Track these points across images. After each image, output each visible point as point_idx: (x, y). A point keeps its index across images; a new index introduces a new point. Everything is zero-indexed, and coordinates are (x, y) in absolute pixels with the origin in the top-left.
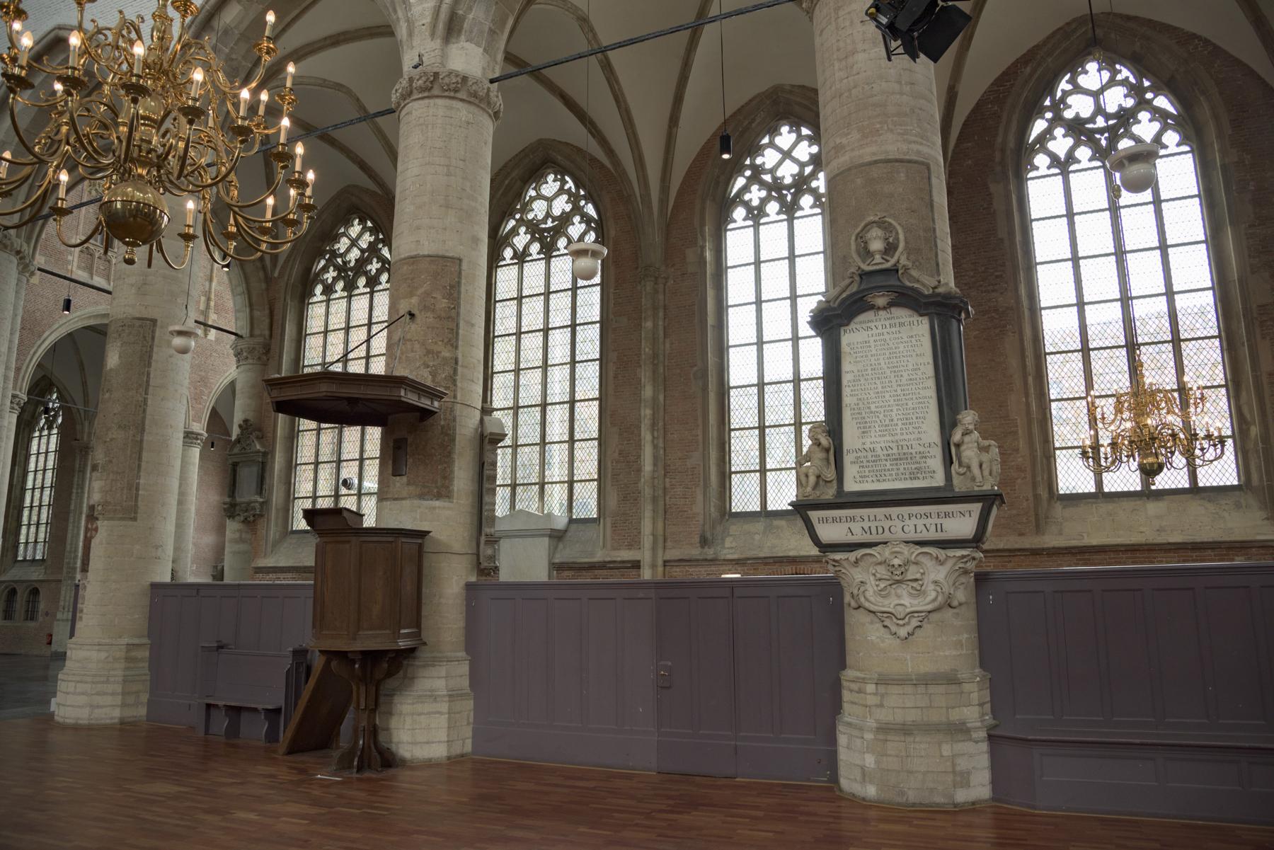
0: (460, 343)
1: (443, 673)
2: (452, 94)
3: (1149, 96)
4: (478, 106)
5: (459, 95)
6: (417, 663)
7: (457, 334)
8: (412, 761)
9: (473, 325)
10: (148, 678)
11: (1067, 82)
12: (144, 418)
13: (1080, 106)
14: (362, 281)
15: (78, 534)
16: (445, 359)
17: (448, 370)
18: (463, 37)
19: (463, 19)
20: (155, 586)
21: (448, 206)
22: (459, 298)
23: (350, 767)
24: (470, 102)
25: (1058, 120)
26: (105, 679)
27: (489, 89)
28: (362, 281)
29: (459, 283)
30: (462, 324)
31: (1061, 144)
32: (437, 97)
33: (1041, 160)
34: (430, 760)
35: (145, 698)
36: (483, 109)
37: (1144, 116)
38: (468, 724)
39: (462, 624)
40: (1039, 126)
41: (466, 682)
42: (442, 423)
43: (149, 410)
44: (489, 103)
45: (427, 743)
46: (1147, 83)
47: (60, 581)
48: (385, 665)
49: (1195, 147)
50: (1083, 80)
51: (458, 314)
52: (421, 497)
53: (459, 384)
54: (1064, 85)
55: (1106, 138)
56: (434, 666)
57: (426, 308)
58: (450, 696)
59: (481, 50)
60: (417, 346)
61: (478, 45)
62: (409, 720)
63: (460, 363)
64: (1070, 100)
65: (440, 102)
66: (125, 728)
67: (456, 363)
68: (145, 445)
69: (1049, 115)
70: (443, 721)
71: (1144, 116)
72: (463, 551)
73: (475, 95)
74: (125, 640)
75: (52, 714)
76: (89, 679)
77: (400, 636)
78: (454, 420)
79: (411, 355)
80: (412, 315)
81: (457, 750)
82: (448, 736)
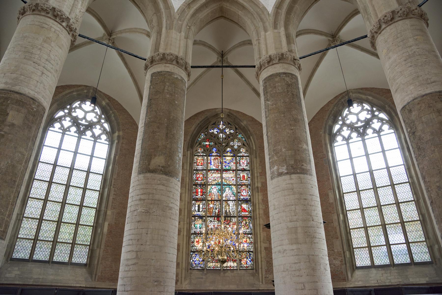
3: (103, 121)
11: (78, 104)
13: (79, 113)
25: (70, 114)
31: (67, 123)
37: (98, 127)
40: (61, 113)
46: (103, 116)
49: (110, 143)
50: (83, 106)
54: (77, 104)
55: (83, 128)
64: (77, 110)
69: (66, 111)
71: (98, 127)
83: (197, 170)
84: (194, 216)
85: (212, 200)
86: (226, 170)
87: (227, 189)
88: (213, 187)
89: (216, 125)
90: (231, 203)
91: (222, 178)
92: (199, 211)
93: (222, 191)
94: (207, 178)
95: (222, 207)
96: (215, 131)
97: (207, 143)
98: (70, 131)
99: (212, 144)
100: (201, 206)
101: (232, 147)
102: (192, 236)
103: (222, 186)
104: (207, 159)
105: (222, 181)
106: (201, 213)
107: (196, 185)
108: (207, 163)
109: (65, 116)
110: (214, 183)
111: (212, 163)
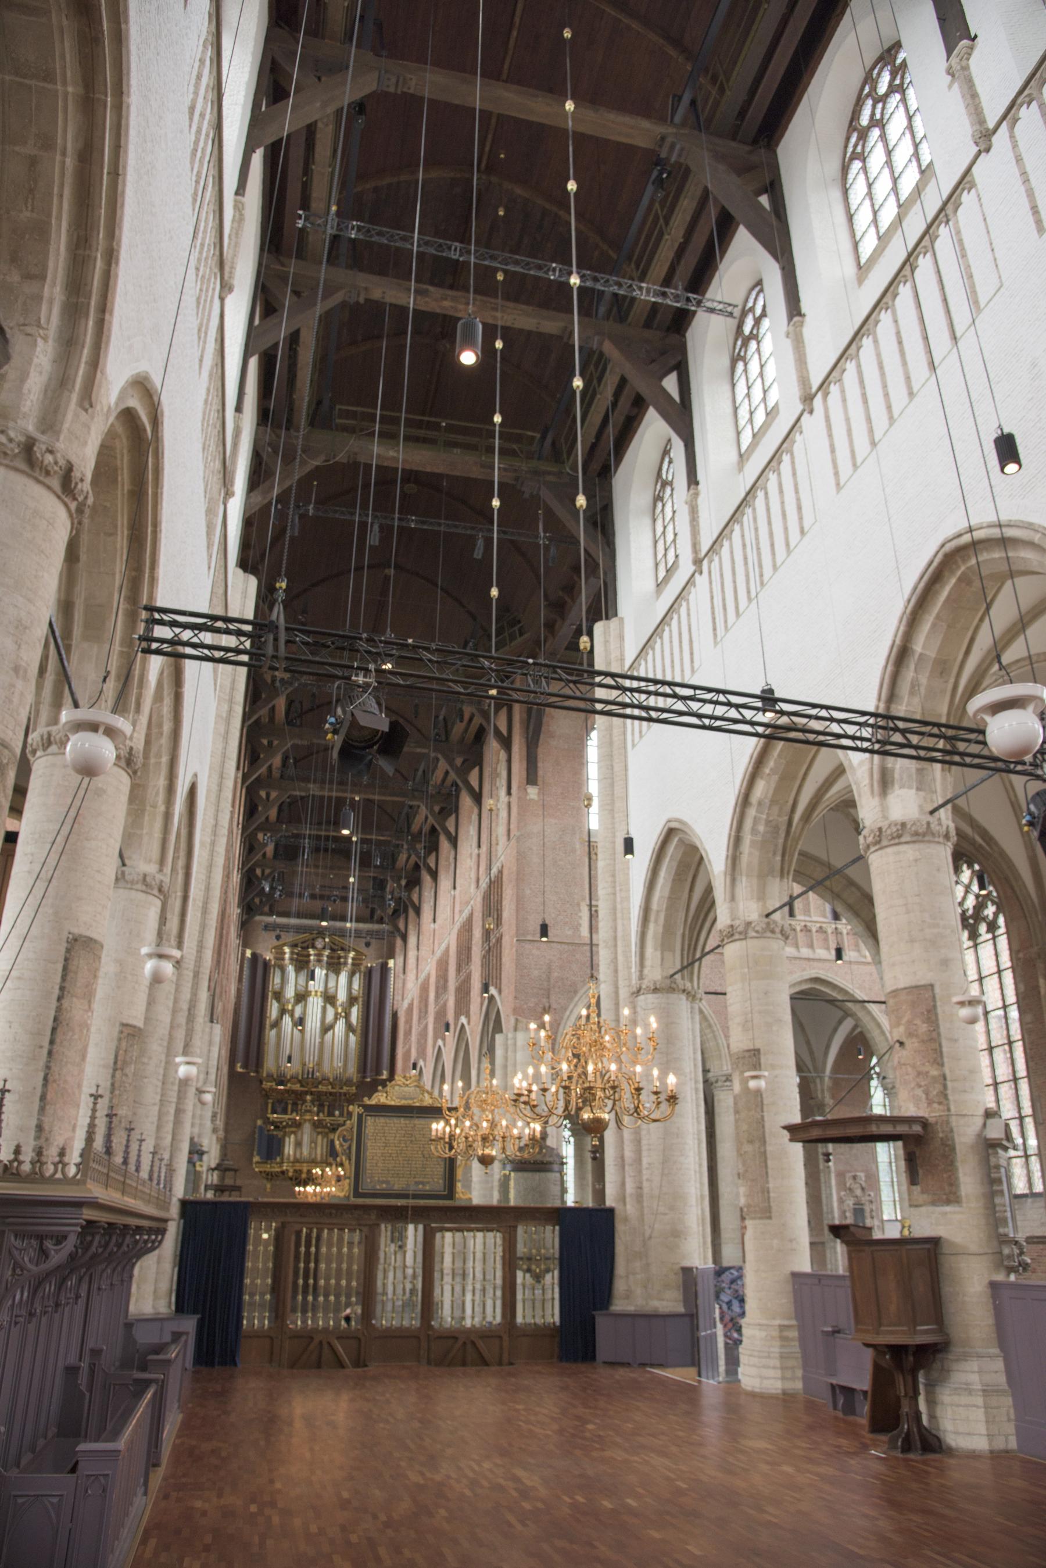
0: (946, 1060)
1: (976, 1369)
2: (897, 841)
4: (922, 841)
5: (903, 839)
6: (950, 1357)
7: (941, 1052)
8: (957, 1450)
9: (956, 1041)
10: (799, 1355)
12: (764, 1132)
14: (983, 928)
15: (831, 1194)
16: (934, 1077)
17: (939, 1087)
18: (896, 786)
19: (893, 770)
20: (795, 1275)
21: (912, 941)
22: (937, 1019)
23: (895, 1448)
24: (914, 842)
26: (766, 1354)
27: (928, 823)
28: (983, 928)
29: (935, 1007)
30: (944, 1043)
32: (886, 847)
34: (974, 1451)
35: (799, 1373)
36: (929, 842)
38: (1009, 1420)
39: (991, 1321)
41: (1002, 1379)
42: (941, 1135)
43: (767, 1125)
44: (933, 834)
45: (969, 1434)
47: (823, 1243)
48: (911, 1358)
51: (939, 1034)
52: (934, 1203)
53: (950, 1097)
56: (966, 1360)
57: (910, 1035)
58: (984, 1391)
59: (914, 791)
60: (910, 1069)
61: (910, 787)
62: (949, 1409)
63: (948, 1077)
65: (889, 850)
66: (787, 1398)
67: (945, 1079)
68: (768, 1156)
70: (980, 1414)
72: (981, 1251)
73: (916, 834)
74: (777, 1322)
75: (739, 1381)
76: (756, 1354)
77: (915, 1332)
78: (952, 1131)
79: (907, 1077)
80: (901, 1044)
81: (1000, 1444)
82: (987, 1429)
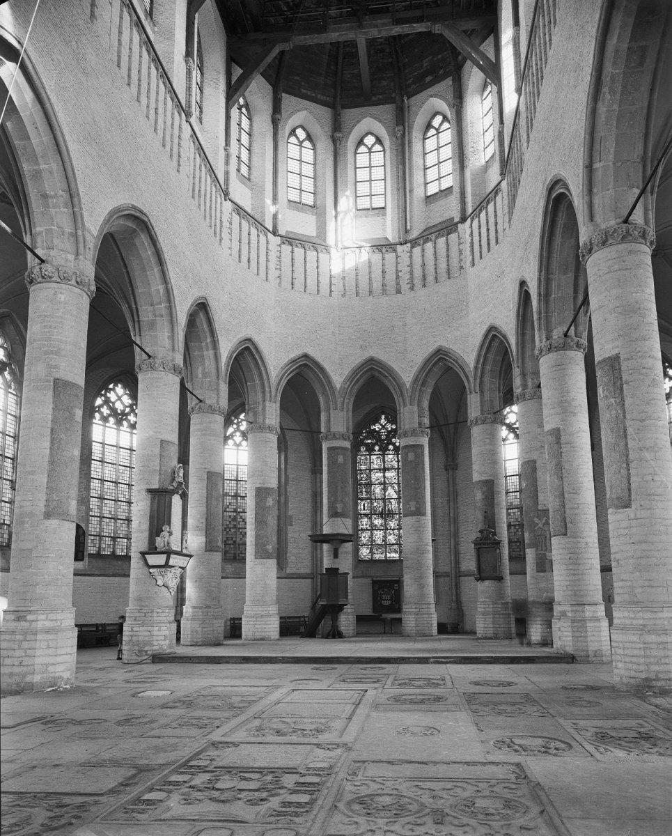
33: (230, 442)
69: (235, 426)
83: (361, 470)
84: (361, 515)
85: (375, 499)
86: (388, 469)
87: (389, 488)
88: (377, 486)
89: (377, 421)
90: (393, 501)
91: (384, 477)
92: (364, 510)
93: (385, 489)
94: (370, 477)
95: (385, 506)
96: (377, 427)
97: (369, 441)
98: (241, 445)
99: (374, 441)
100: (366, 505)
101: (394, 444)
102: (360, 532)
103: (384, 485)
104: (370, 457)
105: (384, 481)
106: (368, 512)
107: (360, 485)
108: (370, 463)
109: (235, 431)
110: (377, 482)
111: (375, 463)
